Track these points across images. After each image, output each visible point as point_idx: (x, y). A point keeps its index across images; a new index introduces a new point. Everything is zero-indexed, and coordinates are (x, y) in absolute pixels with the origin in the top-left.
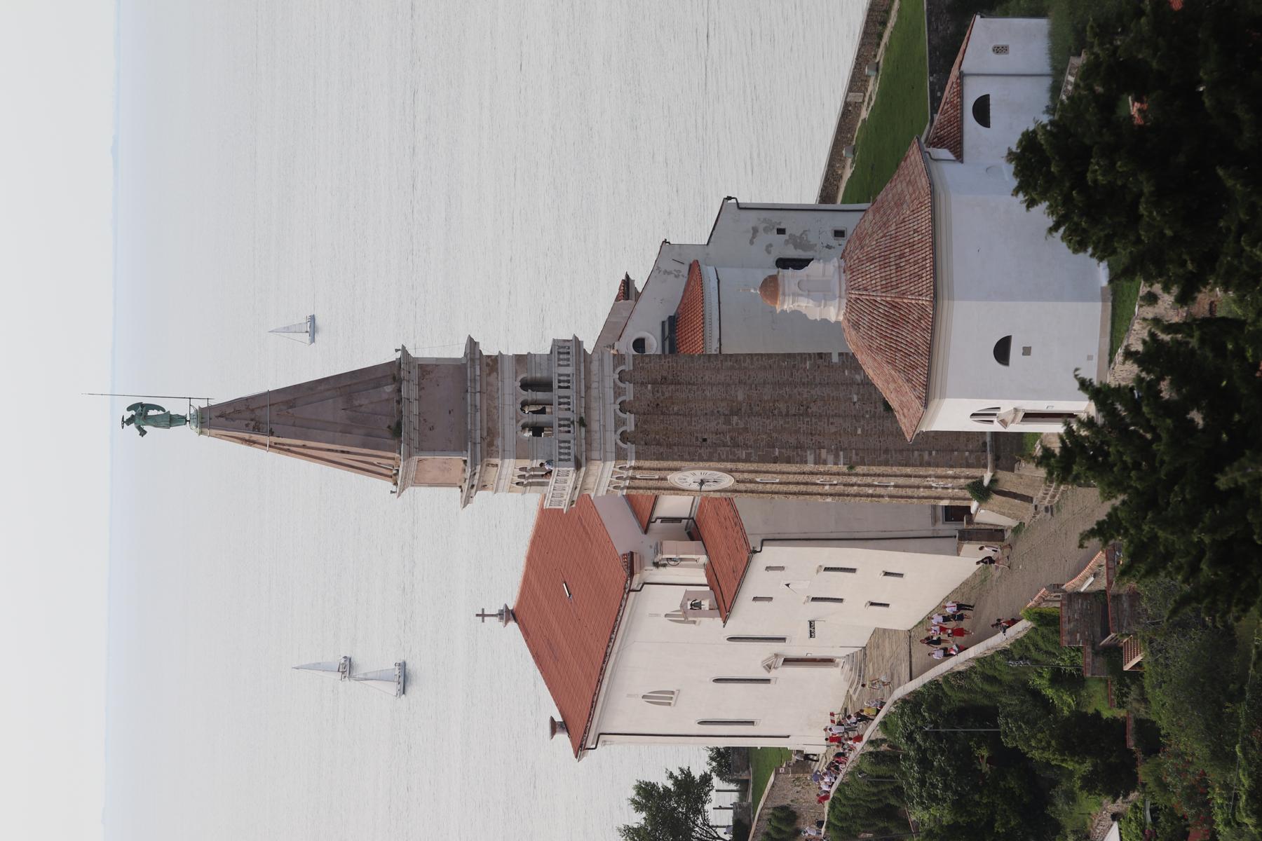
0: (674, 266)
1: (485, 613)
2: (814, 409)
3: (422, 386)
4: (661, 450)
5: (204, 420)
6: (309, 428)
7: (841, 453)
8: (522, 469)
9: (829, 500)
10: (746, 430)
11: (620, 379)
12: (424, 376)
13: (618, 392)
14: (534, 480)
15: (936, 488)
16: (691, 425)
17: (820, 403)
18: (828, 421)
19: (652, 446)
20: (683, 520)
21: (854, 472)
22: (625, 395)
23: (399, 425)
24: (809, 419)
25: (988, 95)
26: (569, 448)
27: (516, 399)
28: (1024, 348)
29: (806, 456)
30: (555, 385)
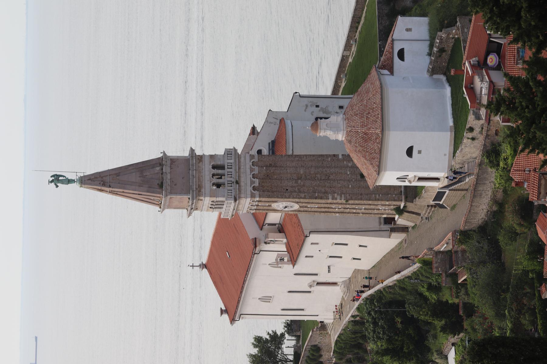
0: (273, 120)
1: (194, 265)
2: (332, 177)
3: (172, 167)
5: (82, 181)
6: (125, 185)
7: (343, 195)
8: (212, 202)
9: (337, 215)
10: (304, 185)
11: (253, 165)
12: (172, 163)
13: (252, 170)
14: (217, 206)
15: (381, 210)
16: (282, 184)
17: (334, 175)
18: (338, 182)
19: (266, 192)
20: (277, 225)
21: (348, 203)
22: (254, 171)
23: (162, 183)
24: (330, 181)
25: (404, 48)
26: (232, 193)
27: (210, 173)
28: (419, 151)
29: (328, 196)
30: (226, 167)
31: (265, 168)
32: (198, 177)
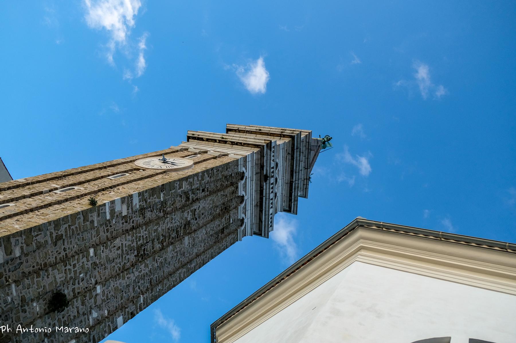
4: (227, 172)
7: (108, 217)
18: (122, 250)
24: (139, 243)
29: (140, 202)
31: (231, 222)
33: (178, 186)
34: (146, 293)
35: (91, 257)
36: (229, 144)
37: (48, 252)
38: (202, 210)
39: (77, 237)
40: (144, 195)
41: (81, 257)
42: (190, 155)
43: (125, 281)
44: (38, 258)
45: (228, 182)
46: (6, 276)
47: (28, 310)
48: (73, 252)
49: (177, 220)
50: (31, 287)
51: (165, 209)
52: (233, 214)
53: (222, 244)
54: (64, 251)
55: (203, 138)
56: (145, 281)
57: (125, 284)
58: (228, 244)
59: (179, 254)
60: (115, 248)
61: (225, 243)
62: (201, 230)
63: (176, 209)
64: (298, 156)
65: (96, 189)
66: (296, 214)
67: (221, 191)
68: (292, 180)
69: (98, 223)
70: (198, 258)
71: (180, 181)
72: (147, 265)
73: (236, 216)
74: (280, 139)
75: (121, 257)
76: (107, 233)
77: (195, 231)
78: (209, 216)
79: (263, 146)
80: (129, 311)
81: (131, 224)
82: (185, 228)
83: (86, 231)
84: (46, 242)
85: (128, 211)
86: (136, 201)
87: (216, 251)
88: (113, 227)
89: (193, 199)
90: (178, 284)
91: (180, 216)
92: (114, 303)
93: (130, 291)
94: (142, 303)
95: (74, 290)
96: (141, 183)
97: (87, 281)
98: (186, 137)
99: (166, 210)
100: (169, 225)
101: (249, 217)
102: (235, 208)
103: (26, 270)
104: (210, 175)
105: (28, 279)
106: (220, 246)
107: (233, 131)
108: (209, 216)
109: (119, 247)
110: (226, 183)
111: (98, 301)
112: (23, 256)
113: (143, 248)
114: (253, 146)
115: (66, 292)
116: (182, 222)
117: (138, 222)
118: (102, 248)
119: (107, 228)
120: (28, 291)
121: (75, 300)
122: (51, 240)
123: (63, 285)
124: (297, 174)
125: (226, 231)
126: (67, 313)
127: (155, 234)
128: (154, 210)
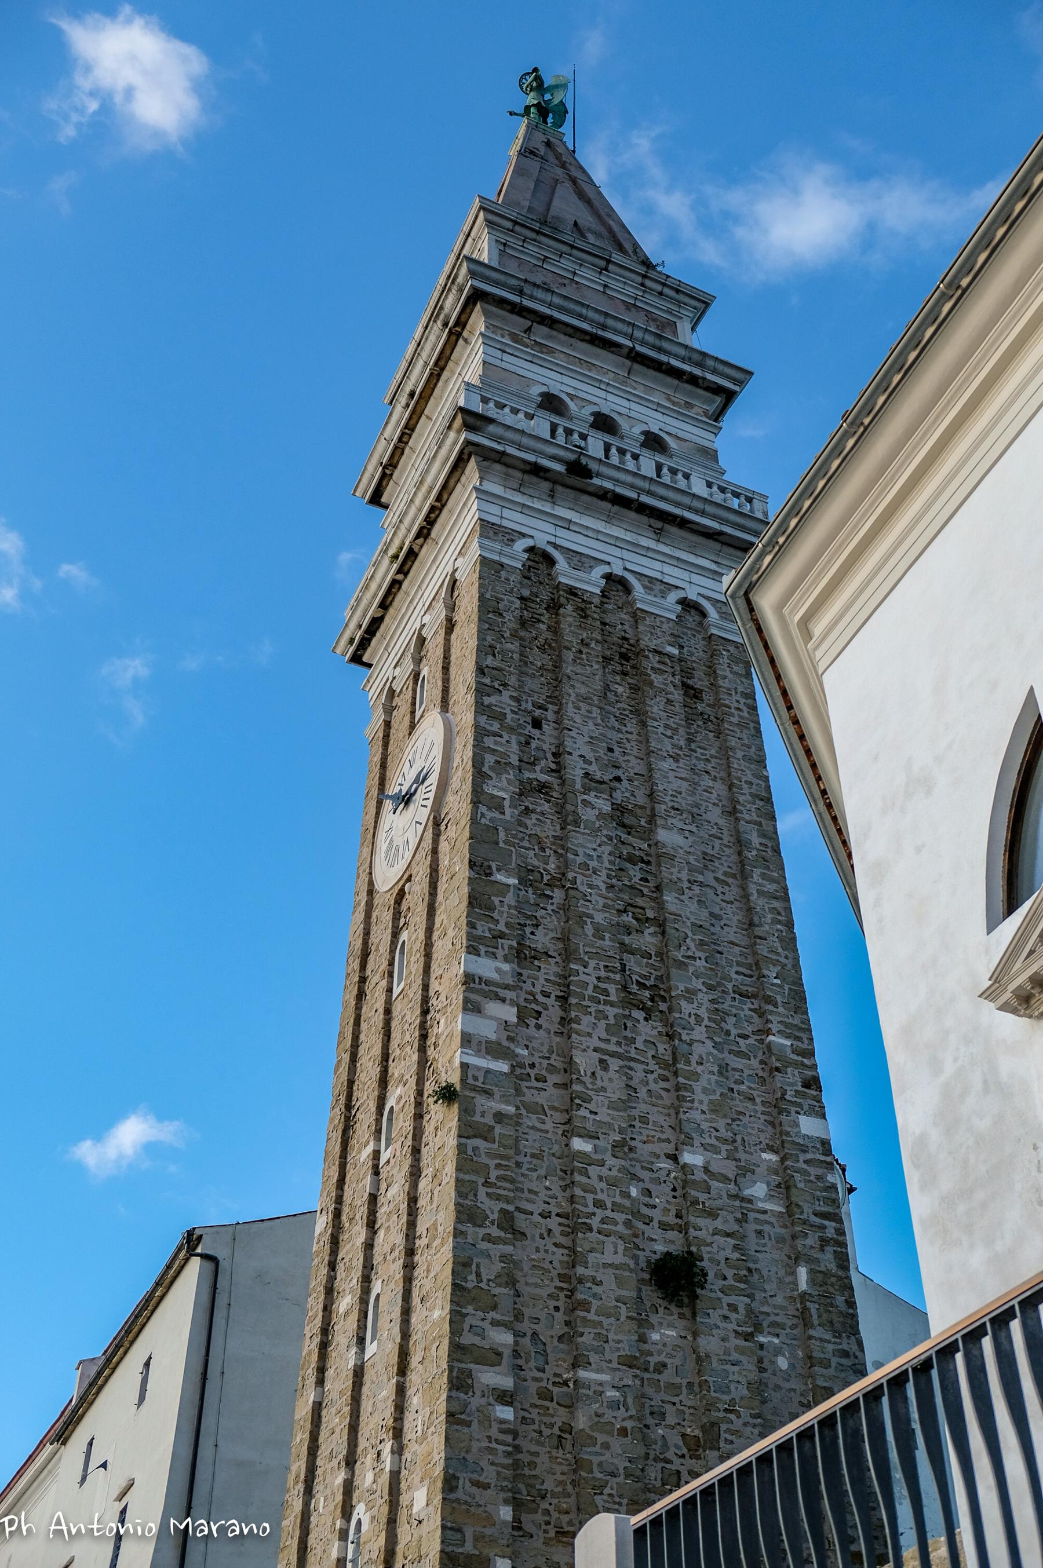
4: (508, 616)
7: (503, 1067)
18: (613, 1055)
24: (613, 998)
31: (675, 651)
32: (594, 365)
33: (493, 815)
34: (768, 1021)
35: (596, 1152)
36: (422, 546)
37: (534, 1260)
38: (597, 752)
39: (523, 1170)
40: (481, 938)
41: (583, 1179)
42: (414, 698)
43: (705, 1077)
44: (537, 1291)
45: (542, 618)
46: (550, 1382)
47: (662, 1358)
48: (560, 1194)
49: (595, 850)
50: (605, 1333)
51: (546, 878)
52: (652, 633)
53: (733, 710)
54: (550, 1217)
55: (374, 618)
56: (734, 1011)
57: (714, 1078)
58: (740, 689)
59: (700, 878)
60: (600, 1073)
61: (735, 698)
62: (657, 776)
63: (561, 840)
64: (548, 297)
65: (415, 1057)
66: (751, 374)
67: (559, 656)
68: (625, 351)
69: (508, 1103)
70: (741, 812)
71: (480, 802)
72: (687, 990)
73: (665, 627)
74: (466, 341)
75: (632, 1064)
76: (546, 1081)
77: (651, 795)
78: (624, 729)
79: (468, 443)
80: (796, 1091)
81: (551, 1001)
82: (628, 828)
83: (517, 1140)
84: (503, 1258)
85: (508, 1002)
86: (488, 968)
87: (746, 742)
88: (537, 1061)
89: (552, 771)
90: (788, 910)
91: (588, 835)
92: (751, 1125)
93: (740, 1067)
94: (792, 1045)
95: (664, 1226)
96: (444, 916)
97: (657, 1181)
98: (354, 666)
99: (549, 877)
100: (600, 881)
101: (685, 575)
102: (636, 621)
103: (559, 1329)
104: (497, 686)
105: (582, 1335)
106: (735, 720)
107: (384, 484)
108: (624, 729)
109: (602, 1061)
110: (543, 627)
111: (723, 1172)
112: (519, 1326)
113: (634, 988)
114: (457, 474)
115: (660, 1248)
116: (607, 836)
117: (552, 978)
118: (583, 1112)
119: (533, 1078)
120: (611, 1343)
121: (692, 1232)
122: (505, 1243)
123: (639, 1249)
124: (610, 322)
125: (699, 680)
126: (719, 1263)
127: (607, 935)
128: (536, 917)
